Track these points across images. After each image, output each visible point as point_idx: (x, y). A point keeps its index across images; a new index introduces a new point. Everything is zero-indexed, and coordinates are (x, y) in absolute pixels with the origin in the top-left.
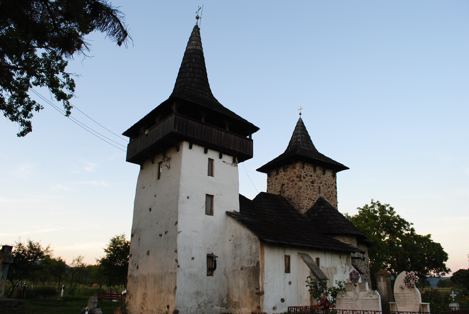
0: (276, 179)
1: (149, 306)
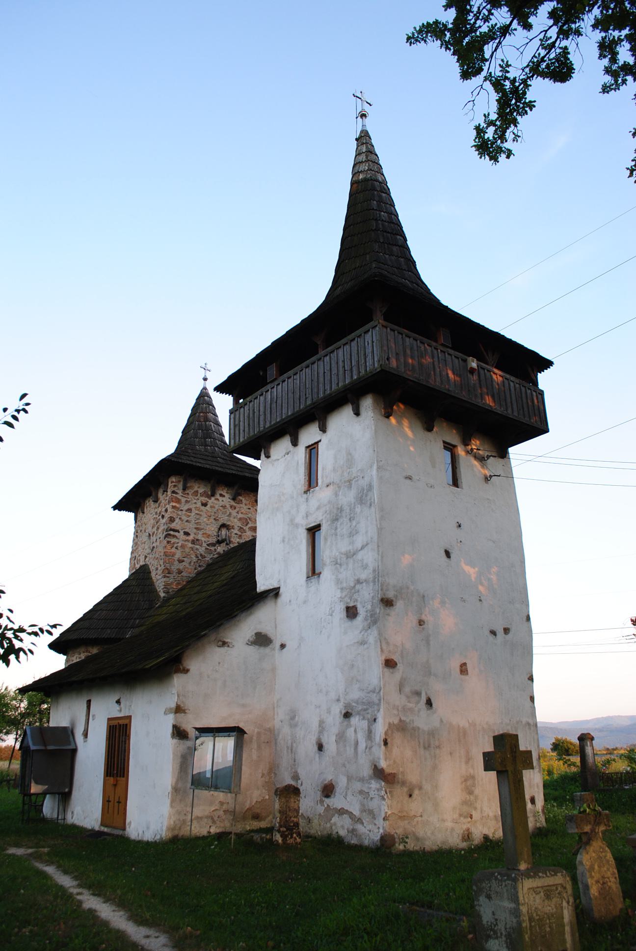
0: (205, 505)
1: (485, 809)
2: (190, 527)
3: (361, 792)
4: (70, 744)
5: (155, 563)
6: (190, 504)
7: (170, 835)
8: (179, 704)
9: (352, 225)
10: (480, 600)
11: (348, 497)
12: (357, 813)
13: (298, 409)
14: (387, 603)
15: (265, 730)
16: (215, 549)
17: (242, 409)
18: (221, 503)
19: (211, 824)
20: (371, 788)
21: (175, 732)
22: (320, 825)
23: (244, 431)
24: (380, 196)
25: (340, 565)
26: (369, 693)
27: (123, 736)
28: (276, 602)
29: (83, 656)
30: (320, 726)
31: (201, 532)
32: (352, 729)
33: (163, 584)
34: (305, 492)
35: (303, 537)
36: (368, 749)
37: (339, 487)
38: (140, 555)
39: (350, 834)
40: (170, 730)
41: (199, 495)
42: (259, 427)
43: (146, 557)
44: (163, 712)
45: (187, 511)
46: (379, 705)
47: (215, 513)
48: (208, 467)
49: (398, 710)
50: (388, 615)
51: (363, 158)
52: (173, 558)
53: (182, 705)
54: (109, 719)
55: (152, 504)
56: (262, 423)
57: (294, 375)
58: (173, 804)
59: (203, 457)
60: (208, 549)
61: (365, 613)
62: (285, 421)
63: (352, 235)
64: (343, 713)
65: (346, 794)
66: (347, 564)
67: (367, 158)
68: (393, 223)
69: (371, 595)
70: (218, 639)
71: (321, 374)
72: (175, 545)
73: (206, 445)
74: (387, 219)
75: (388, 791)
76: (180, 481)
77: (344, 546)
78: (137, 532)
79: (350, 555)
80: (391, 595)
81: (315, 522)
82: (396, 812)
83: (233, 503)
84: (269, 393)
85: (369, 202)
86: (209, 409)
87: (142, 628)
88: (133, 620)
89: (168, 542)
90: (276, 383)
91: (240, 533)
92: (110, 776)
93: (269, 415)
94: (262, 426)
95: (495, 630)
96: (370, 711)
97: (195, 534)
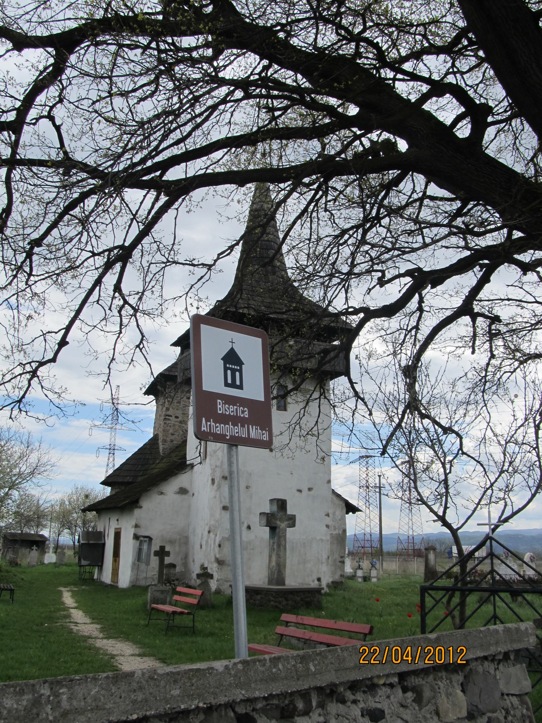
40: (132, 536)
54: (115, 529)
87: (146, 476)
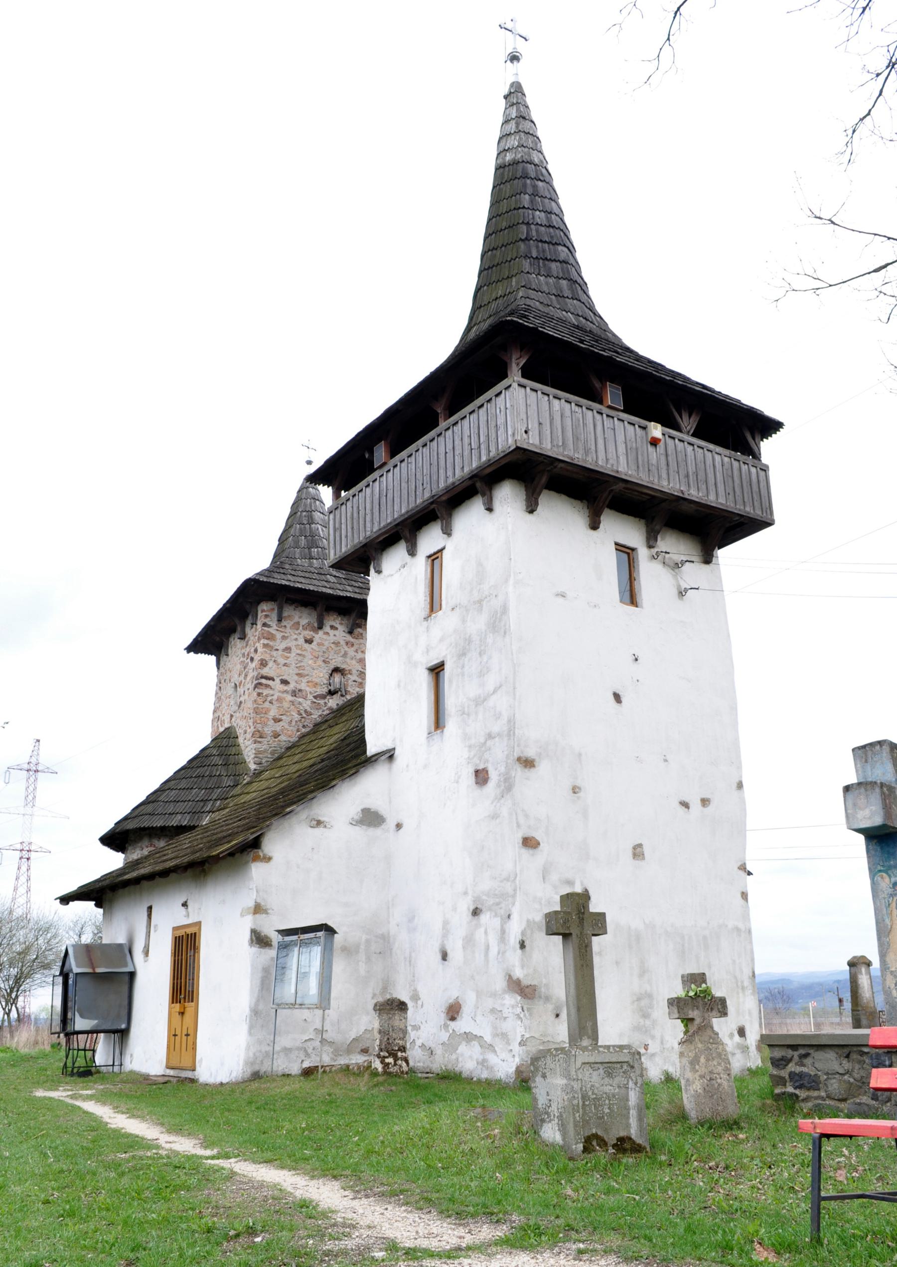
0: (309, 641)
2: (289, 674)
3: (493, 1011)
4: (126, 965)
5: (242, 723)
6: (288, 640)
7: (249, 1070)
8: (258, 901)
9: (493, 233)
10: (666, 761)
11: (478, 624)
12: (488, 1038)
13: (413, 505)
14: (528, 763)
15: (376, 937)
16: (325, 703)
17: (344, 507)
18: (332, 639)
19: (304, 1058)
20: (504, 1004)
21: (254, 938)
22: (444, 1057)
23: (347, 536)
24: (535, 187)
25: (468, 715)
26: (502, 881)
27: (191, 949)
28: (390, 769)
29: (146, 852)
30: (443, 928)
31: (304, 680)
32: (482, 930)
33: (254, 752)
34: (426, 619)
35: (424, 680)
36: (500, 955)
37: (467, 610)
38: (224, 715)
39: (480, 1067)
40: (247, 935)
41: (301, 628)
42: (365, 531)
43: (232, 716)
44: (239, 913)
45: (284, 650)
46: (514, 896)
47: (324, 652)
48: (312, 588)
49: (541, 904)
50: (527, 779)
51: (512, 127)
52: (266, 716)
53: (263, 904)
54: (175, 929)
55: (238, 643)
56: (368, 525)
57: (408, 457)
58: (252, 1031)
59: (307, 575)
60: (315, 702)
61: (497, 778)
62: (397, 522)
63: (494, 249)
64: (471, 910)
65: (475, 1015)
66: (476, 713)
67: (517, 127)
68: (553, 227)
69: (506, 753)
70: (311, 817)
71: (442, 456)
72: (269, 699)
73: (311, 558)
74: (545, 222)
75: (525, 1008)
76: (273, 609)
77: (473, 690)
78: (220, 683)
79: (479, 701)
80: (531, 753)
81: (437, 659)
82: (537, 1035)
83: (349, 638)
84: (377, 483)
85: (518, 196)
86: (316, 506)
88: (212, 802)
89: (259, 694)
90: (386, 468)
91: (360, 680)
92: (177, 1003)
93: (377, 513)
94: (368, 529)
95: (687, 800)
96: (503, 905)
97: (296, 682)
